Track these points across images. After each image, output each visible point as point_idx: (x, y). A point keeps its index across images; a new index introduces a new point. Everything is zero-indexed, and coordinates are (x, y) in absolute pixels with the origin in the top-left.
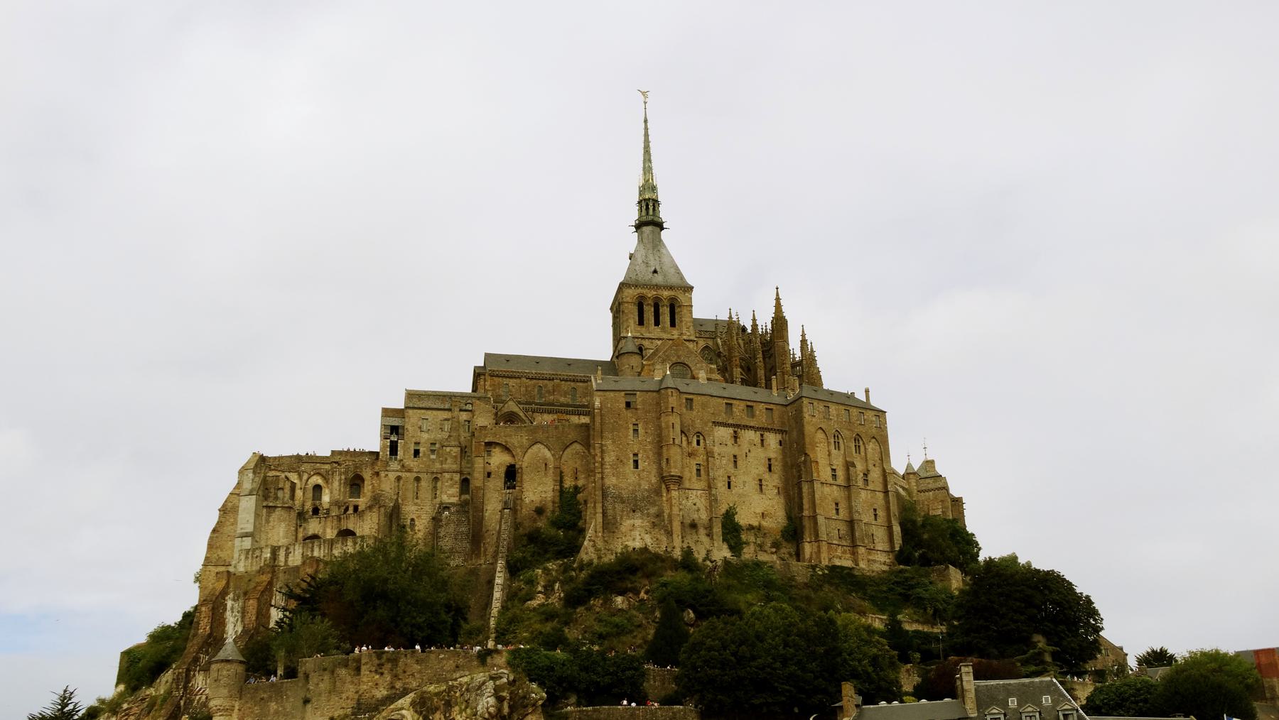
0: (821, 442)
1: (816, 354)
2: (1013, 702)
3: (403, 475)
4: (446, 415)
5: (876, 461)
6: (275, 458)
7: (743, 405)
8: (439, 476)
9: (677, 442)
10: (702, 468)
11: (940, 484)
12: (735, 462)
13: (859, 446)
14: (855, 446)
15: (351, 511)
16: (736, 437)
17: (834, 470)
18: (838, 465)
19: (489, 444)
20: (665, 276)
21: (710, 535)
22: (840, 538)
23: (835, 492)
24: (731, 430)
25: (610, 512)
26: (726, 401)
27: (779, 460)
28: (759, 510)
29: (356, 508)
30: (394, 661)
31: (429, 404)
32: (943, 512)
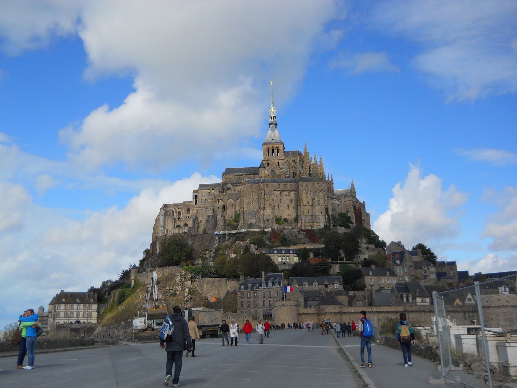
3: (198, 208)
4: (209, 191)
5: (322, 197)
6: (169, 204)
8: (207, 208)
9: (262, 198)
10: (271, 204)
11: (349, 199)
15: (187, 217)
16: (281, 194)
19: (218, 200)
23: (309, 208)
24: (280, 192)
25: (245, 218)
26: (278, 184)
29: (189, 217)
30: (163, 269)
32: (350, 207)
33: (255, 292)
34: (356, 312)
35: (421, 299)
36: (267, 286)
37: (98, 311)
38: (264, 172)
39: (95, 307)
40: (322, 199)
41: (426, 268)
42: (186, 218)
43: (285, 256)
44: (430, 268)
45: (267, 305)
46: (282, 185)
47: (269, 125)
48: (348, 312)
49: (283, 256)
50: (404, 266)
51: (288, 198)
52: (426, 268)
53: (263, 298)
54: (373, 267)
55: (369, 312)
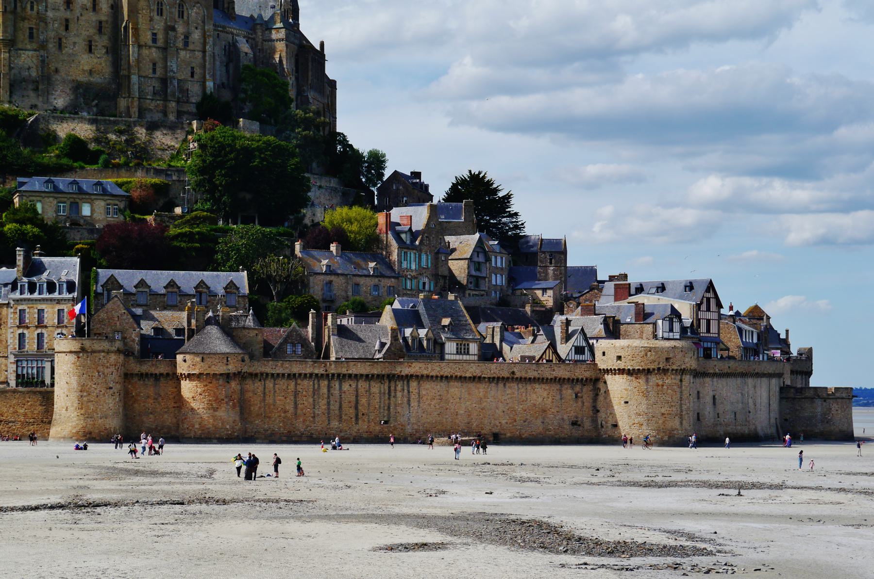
0: (143, 9)
5: (198, 24)
9: (8, 9)
10: (34, 30)
13: (183, 12)
14: (179, 11)
17: (154, 34)
18: (159, 29)
22: (154, 93)
27: (109, 23)
28: (86, 68)
34: (283, 375)
35: (457, 344)
40: (196, 31)
41: (481, 259)
43: (78, 200)
44: (493, 260)
45: (31, 346)
48: (262, 374)
49: (72, 200)
50: (421, 251)
51: (93, 17)
52: (481, 259)
53: (19, 327)
55: (317, 375)
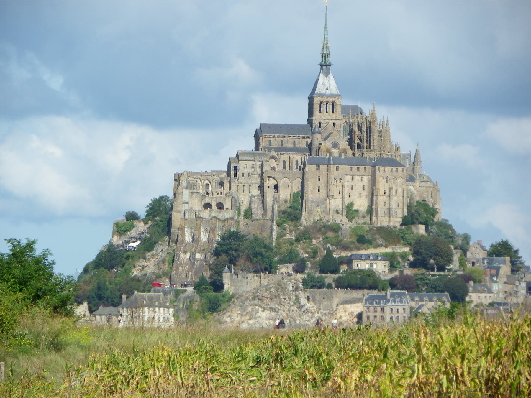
1: (389, 122)
2: (396, 297)
4: (253, 163)
7: (356, 167)
12: (352, 188)
15: (220, 193)
16: (353, 179)
17: (385, 190)
19: (269, 177)
20: (331, 91)
21: (342, 214)
25: (310, 206)
26: (350, 166)
28: (359, 204)
29: (221, 193)
31: (247, 158)
33: (382, 307)
36: (394, 303)
37: (176, 316)
38: (325, 143)
39: (171, 310)
42: (218, 194)
46: (355, 168)
47: (322, 66)
54: (472, 283)
